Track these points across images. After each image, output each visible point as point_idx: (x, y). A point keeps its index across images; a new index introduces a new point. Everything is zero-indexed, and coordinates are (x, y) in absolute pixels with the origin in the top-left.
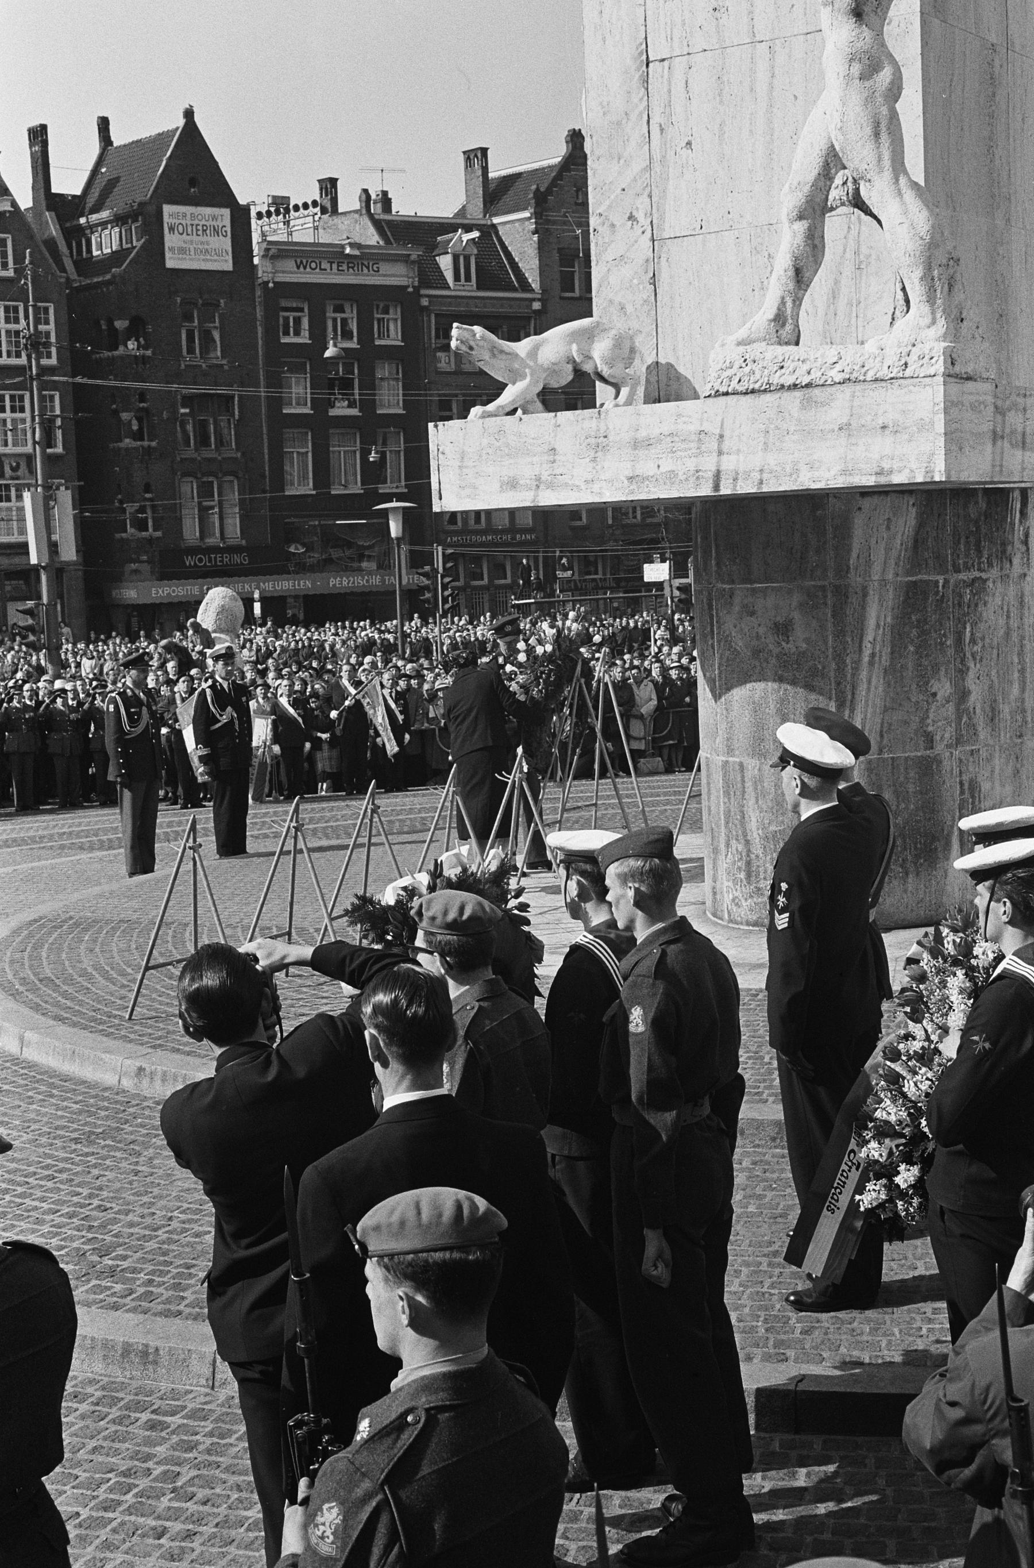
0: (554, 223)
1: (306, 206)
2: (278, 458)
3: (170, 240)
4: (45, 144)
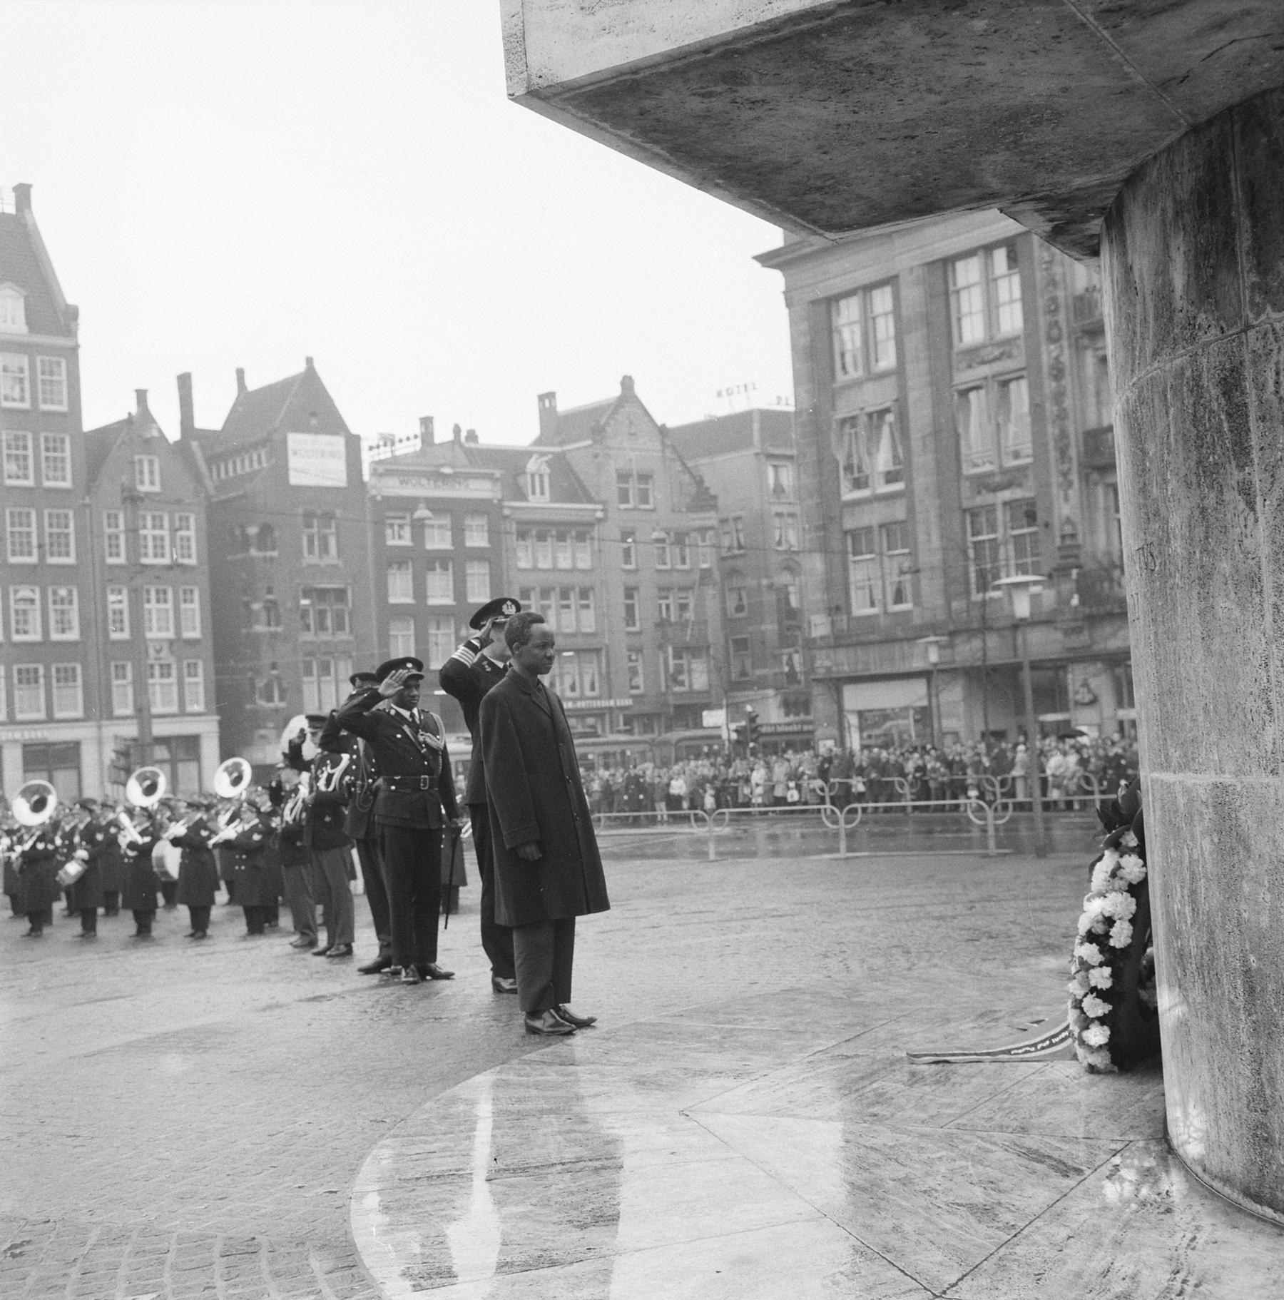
0: (610, 448)
1: (408, 439)
3: (293, 462)
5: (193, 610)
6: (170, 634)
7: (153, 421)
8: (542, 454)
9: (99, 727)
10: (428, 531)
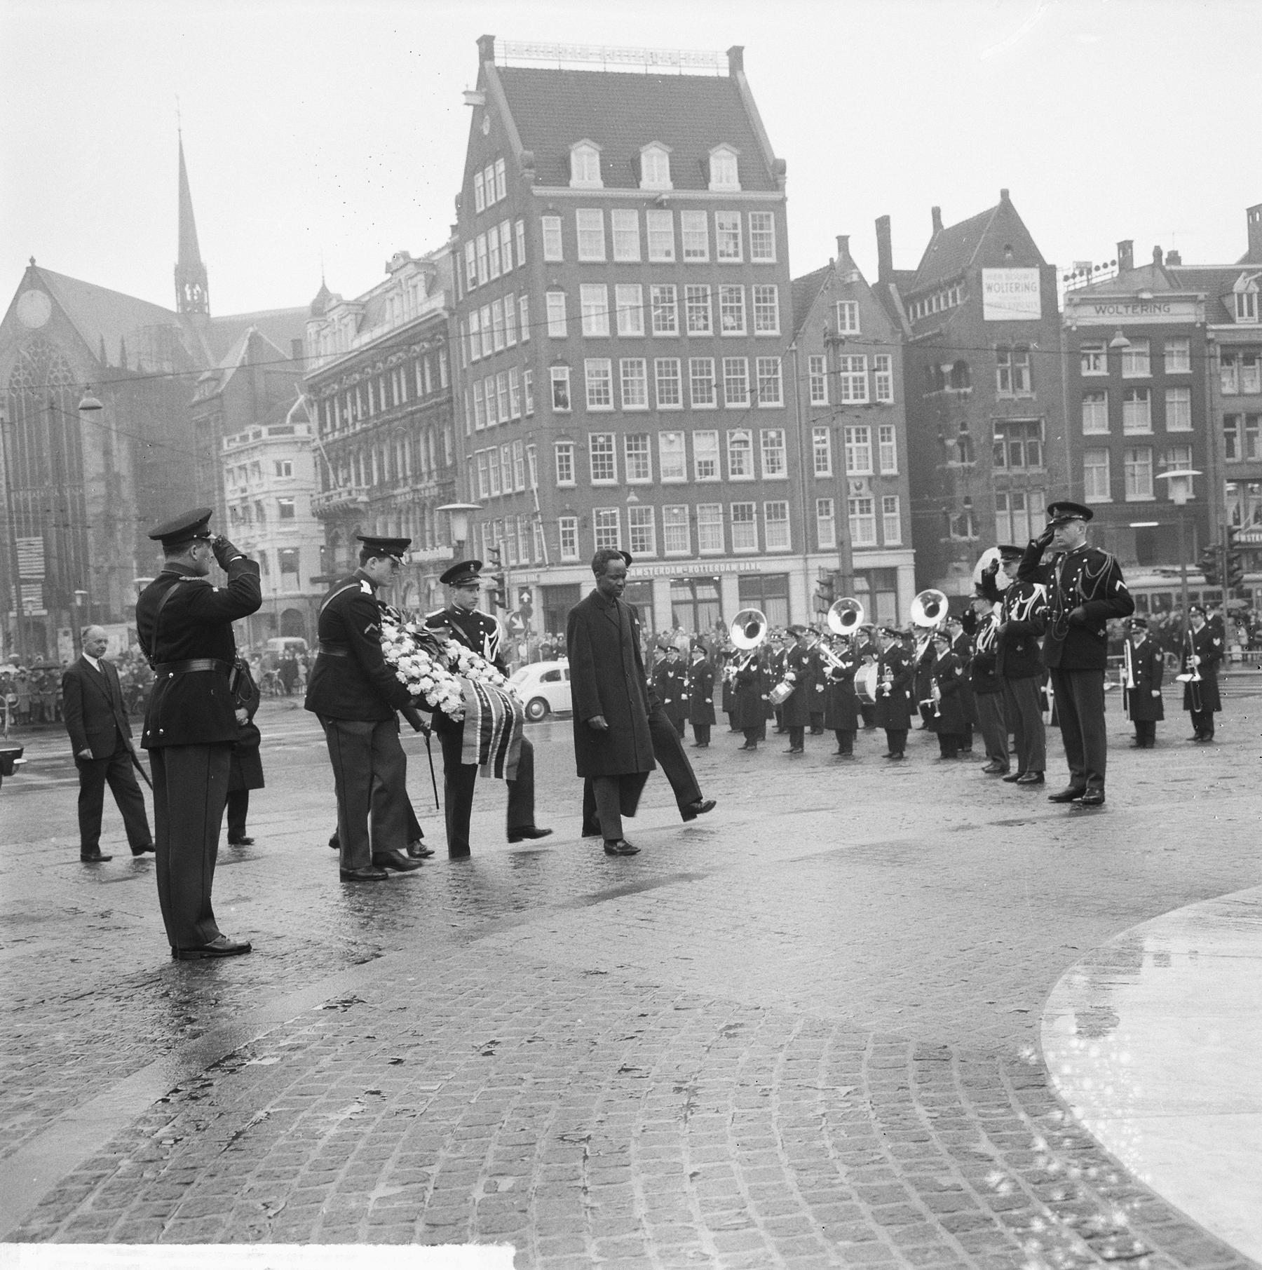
1: (1105, 266)
2: (1079, 472)
3: (988, 297)
4: (889, 230)
5: (891, 447)
6: (870, 472)
7: (854, 266)
8: (1251, 272)
9: (806, 559)
10: (1125, 360)
